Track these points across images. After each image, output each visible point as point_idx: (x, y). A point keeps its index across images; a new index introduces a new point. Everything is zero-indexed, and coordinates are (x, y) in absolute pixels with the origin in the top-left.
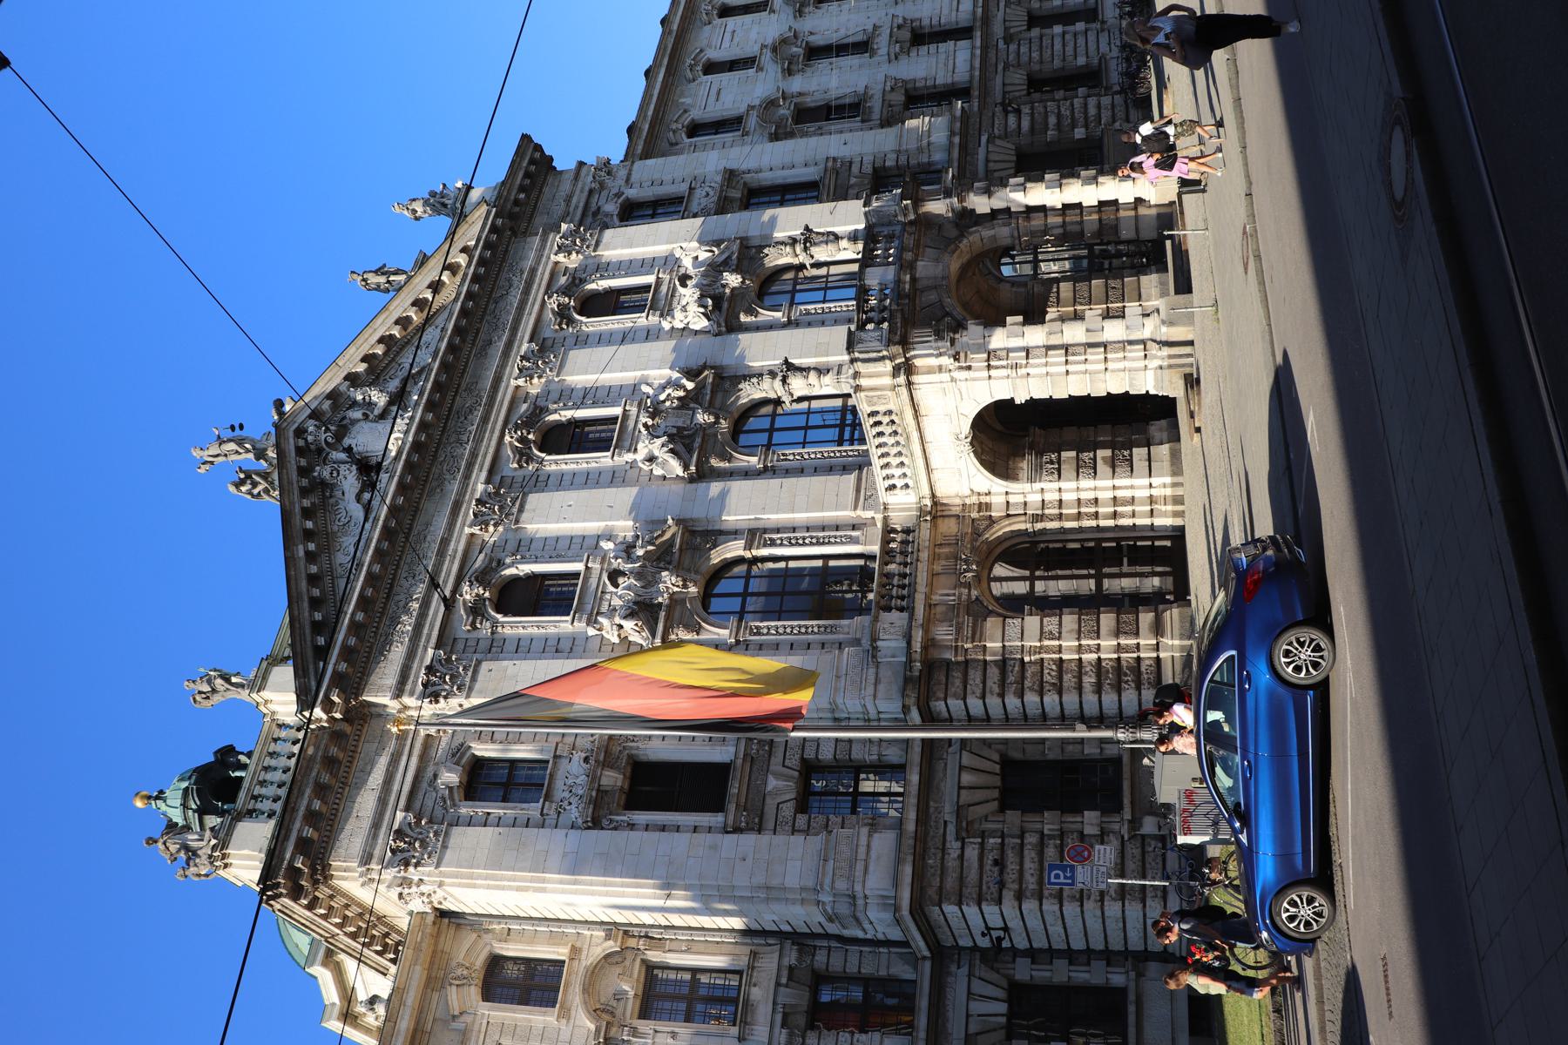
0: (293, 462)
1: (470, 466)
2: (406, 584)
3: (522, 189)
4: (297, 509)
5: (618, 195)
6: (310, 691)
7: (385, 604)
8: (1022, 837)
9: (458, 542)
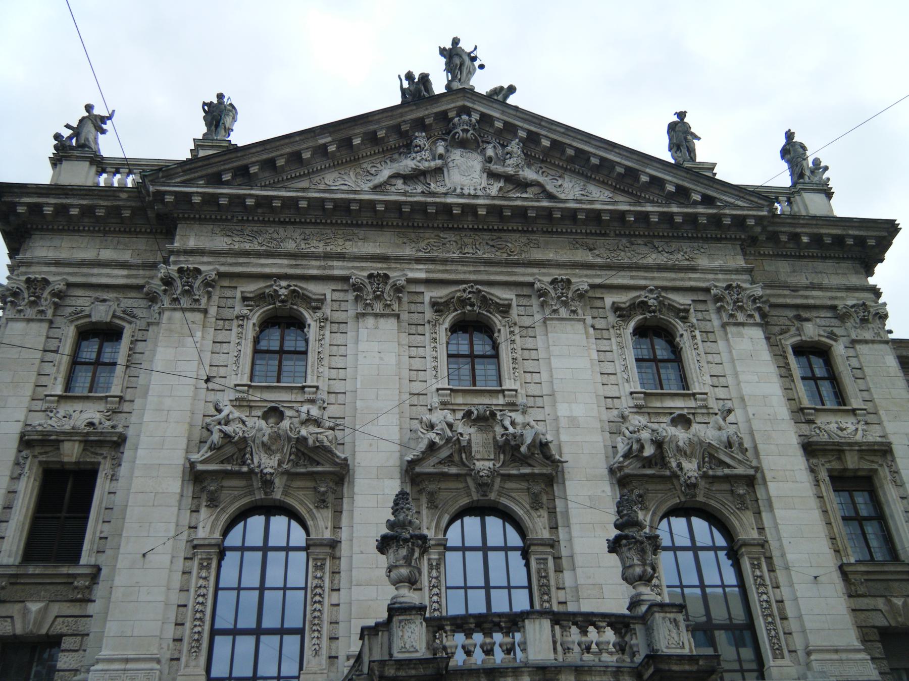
0: (427, 112)
1: (433, 261)
3: (817, 239)
4: (372, 127)
5: (833, 336)
6: (170, 179)
7: (274, 222)
9: (342, 268)
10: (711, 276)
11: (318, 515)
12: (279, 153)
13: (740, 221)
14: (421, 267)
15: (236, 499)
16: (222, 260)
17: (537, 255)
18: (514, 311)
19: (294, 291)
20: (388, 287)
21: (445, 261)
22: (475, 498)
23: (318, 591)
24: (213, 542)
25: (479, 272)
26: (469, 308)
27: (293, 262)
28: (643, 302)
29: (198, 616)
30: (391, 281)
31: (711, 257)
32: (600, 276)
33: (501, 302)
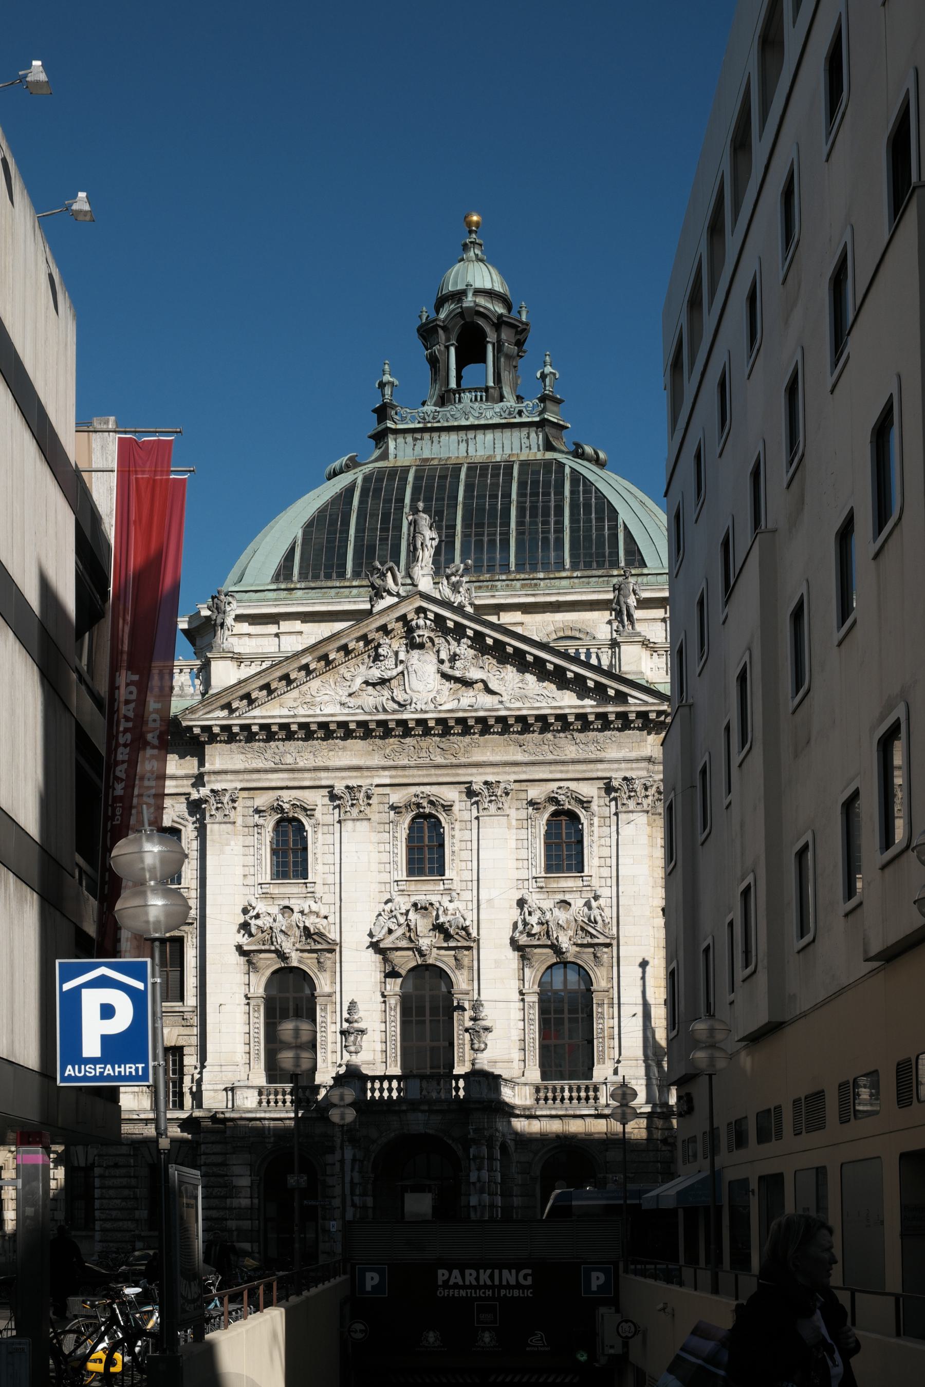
0: (388, 619)
1: (395, 768)
2: (292, 749)
8: (135, 1177)
9: (327, 778)
10: (616, 766)
11: (320, 976)
12: (272, 677)
13: (643, 715)
14: (386, 773)
15: (268, 967)
16: (241, 777)
17: (477, 757)
18: (456, 808)
19: (294, 804)
20: (362, 794)
21: (404, 767)
22: (420, 963)
23: (324, 1025)
24: (259, 995)
25: (430, 775)
26: (421, 810)
27: (291, 775)
28: (554, 797)
29: (256, 1040)
30: (364, 789)
31: (620, 746)
32: (524, 772)
33: (445, 803)
